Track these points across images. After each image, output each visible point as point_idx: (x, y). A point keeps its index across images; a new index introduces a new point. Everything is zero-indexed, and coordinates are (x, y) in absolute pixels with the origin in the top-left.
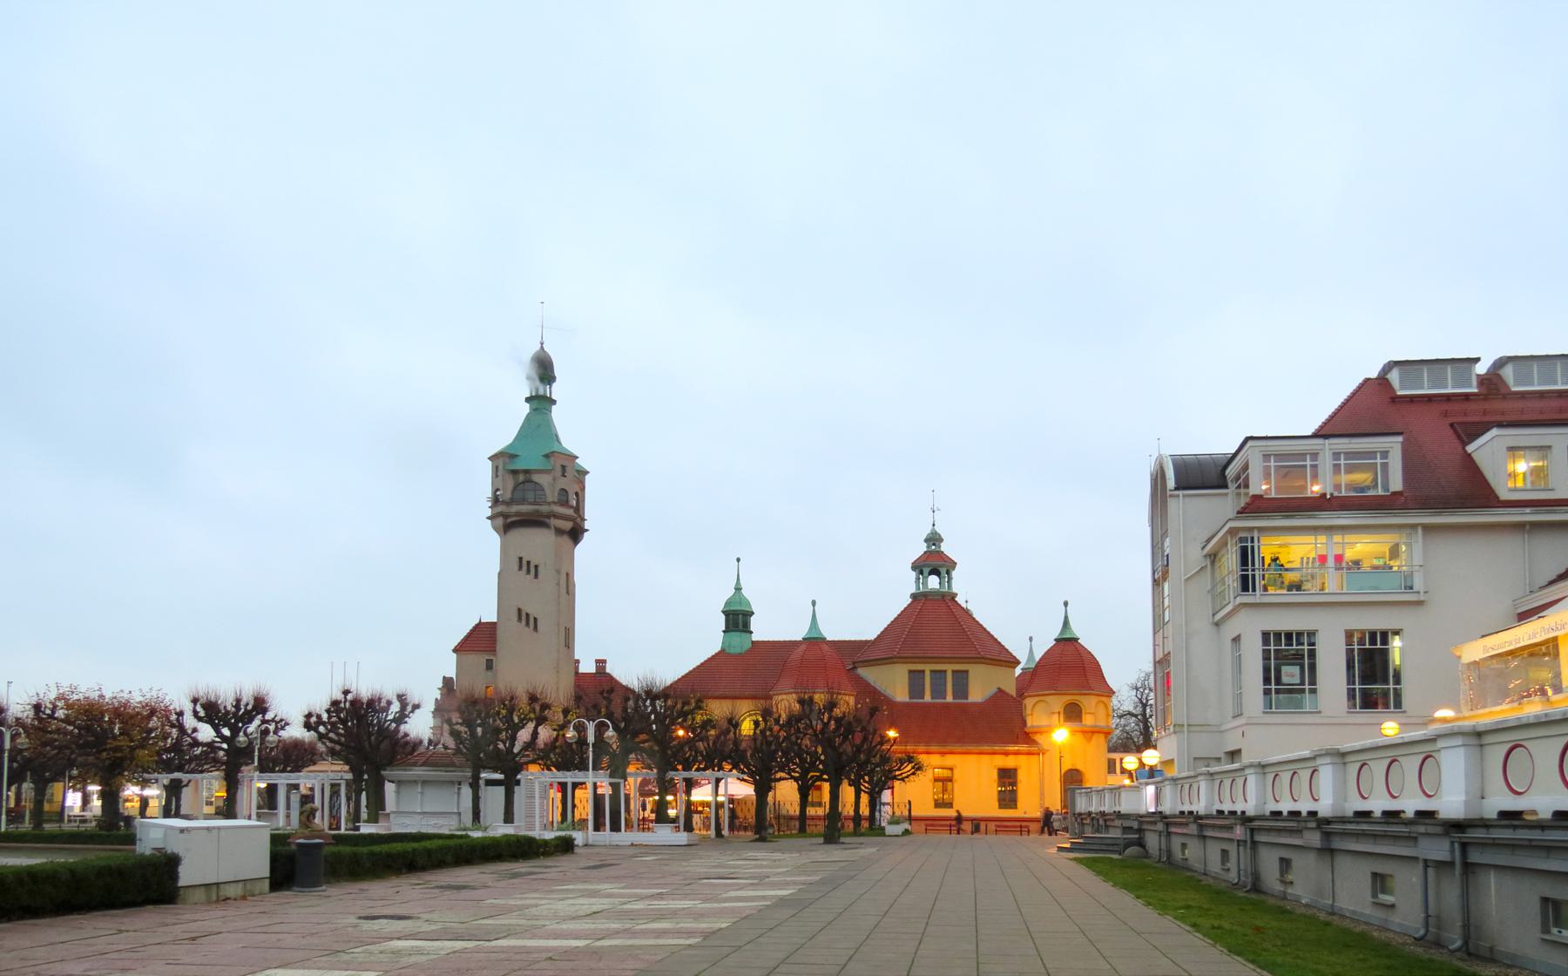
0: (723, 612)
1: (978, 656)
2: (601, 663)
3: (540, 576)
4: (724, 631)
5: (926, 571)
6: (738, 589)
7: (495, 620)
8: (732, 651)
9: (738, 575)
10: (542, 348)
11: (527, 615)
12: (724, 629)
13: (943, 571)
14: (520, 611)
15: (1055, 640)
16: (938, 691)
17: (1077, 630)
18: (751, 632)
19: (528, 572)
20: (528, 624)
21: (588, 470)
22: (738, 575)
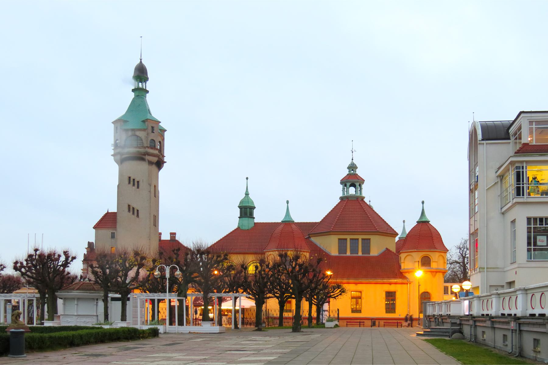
0: (239, 207)
1: (375, 231)
2: (173, 235)
3: (140, 187)
4: (239, 217)
5: (348, 184)
6: (247, 194)
7: (116, 211)
8: (244, 228)
9: (247, 187)
10: (141, 62)
11: (133, 208)
12: (239, 216)
13: (357, 184)
15: (417, 222)
16: (354, 250)
17: (429, 217)
18: (254, 218)
19: (134, 185)
20: (133, 213)
21: (166, 128)
22: (247, 187)
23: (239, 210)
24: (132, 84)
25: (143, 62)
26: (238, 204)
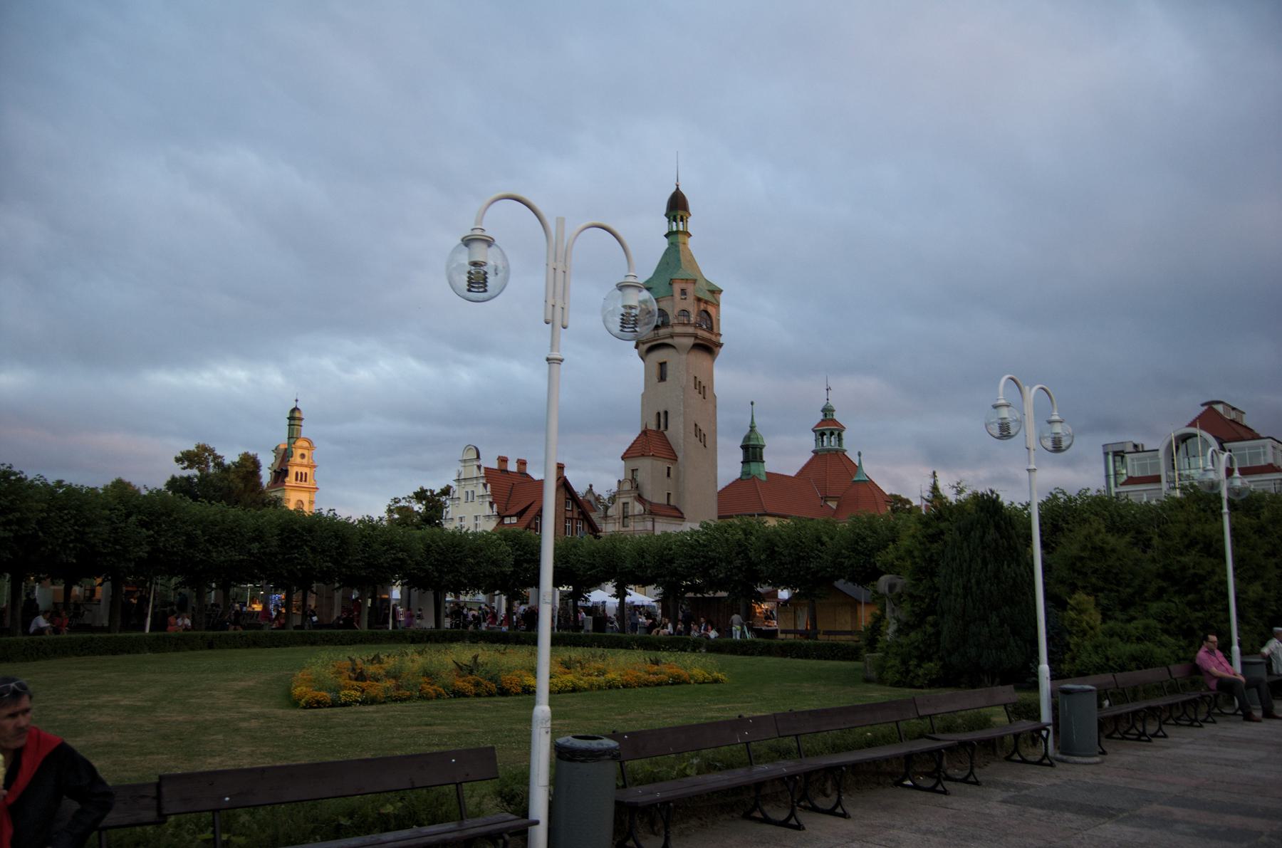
0: (741, 447)
4: (742, 462)
6: (752, 428)
9: (752, 413)
10: (678, 189)
11: (700, 430)
12: (742, 460)
14: (696, 425)
22: (752, 413)
23: (741, 451)
24: (663, 225)
25: (681, 189)
26: (740, 443)
